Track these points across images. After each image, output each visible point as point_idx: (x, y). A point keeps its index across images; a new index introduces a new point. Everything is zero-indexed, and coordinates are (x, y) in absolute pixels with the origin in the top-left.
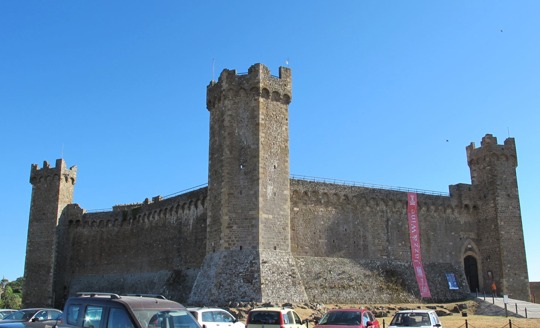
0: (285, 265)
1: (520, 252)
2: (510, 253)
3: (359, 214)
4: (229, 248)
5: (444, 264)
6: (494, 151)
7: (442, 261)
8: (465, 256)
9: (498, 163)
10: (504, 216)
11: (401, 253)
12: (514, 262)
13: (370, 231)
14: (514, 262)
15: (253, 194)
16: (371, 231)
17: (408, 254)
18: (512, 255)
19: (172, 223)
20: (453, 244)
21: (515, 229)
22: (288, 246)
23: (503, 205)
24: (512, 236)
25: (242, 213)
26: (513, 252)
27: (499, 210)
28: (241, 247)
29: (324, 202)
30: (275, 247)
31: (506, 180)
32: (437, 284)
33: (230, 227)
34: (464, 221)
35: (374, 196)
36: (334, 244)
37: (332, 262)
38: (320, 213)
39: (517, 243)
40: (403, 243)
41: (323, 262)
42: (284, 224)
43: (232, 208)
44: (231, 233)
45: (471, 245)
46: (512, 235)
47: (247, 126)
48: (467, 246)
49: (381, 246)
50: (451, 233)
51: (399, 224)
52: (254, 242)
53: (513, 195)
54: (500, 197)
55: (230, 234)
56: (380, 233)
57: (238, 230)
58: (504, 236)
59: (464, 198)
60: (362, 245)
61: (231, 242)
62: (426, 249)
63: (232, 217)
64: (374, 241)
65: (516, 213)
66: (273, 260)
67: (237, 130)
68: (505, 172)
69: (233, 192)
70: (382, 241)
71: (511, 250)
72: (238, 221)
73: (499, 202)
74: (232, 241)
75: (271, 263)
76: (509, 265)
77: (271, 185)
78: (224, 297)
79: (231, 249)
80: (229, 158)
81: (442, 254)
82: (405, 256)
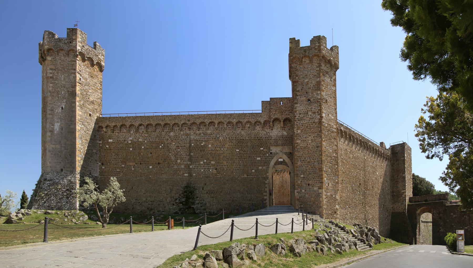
1: (316, 161)
2: (305, 162)
6: (294, 56)
9: (301, 68)
10: (302, 124)
11: (202, 170)
12: (309, 172)
14: (309, 172)
17: (210, 170)
18: (306, 164)
21: (313, 136)
23: (301, 112)
24: (308, 144)
26: (308, 161)
27: (297, 117)
31: (307, 83)
39: (314, 152)
46: (309, 144)
53: (313, 100)
54: (299, 104)
58: (299, 145)
64: (177, 161)
65: (315, 119)
68: (307, 75)
70: (184, 161)
71: (306, 159)
73: (297, 109)
76: (302, 176)
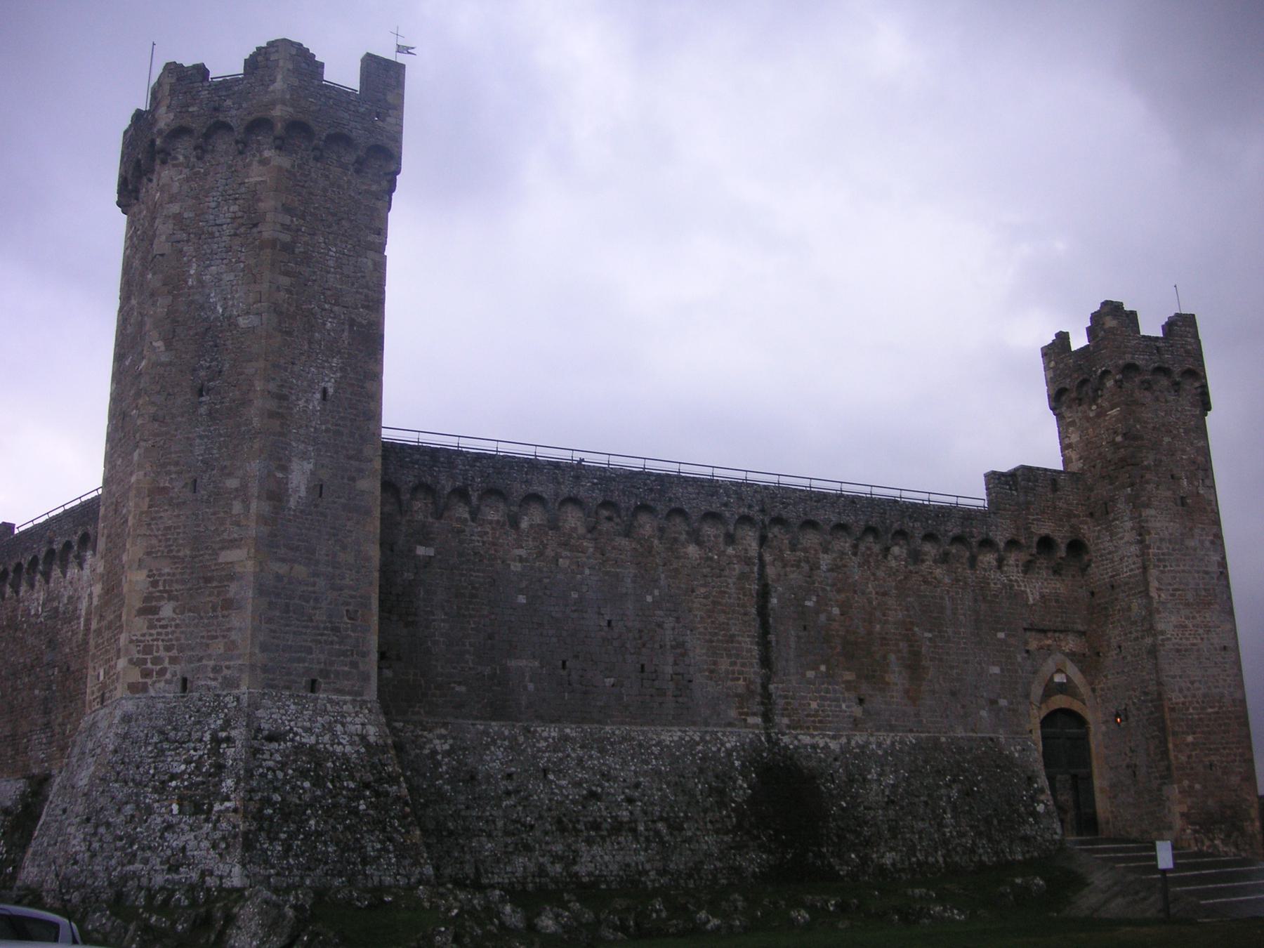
0: (348, 749)
3: (661, 569)
4: (144, 688)
5: (970, 739)
7: (966, 731)
8: (1044, 713)
13: (702, 630)
15: (237, 490)
16: (706, 629)
17: (840, 706)
19: (33, 612)
20: (1002, 670)
22: (365, 678)
25: (193, 557)
28: (185, 680)
29: (531, 526)
30: (314, 682)
32: (945, 812)
33: (148, 610)
34: (1040, 593)
35: (715, 507)
36: (564, 673)
37: (554, 738)
38: (516, 567)
40: (823, 668)
41: (521, 739)
42: (352, 597)
43: (160, 541)
44: (154, 632)
45: (1063, 675)
47: (227, 252)
48: (1052, 678)
49: (741, 682)
50: (996, 635)
51: (808, 603)
52: (232, 663)
55: (151, 635)
56: (738, 635)
57: (178, 622)
59: (1037, 514)
60: (669, 677)
61: (152, 663)
62: (907, 692)
63: (160, 575)
64: (715, 663)
66: (300, 730)
67: (194, 266)
69: (167, 485)
70: (743, 665)
72: (179, 587)
74: (156, 661)
75: (292, 740)
77: (304, 456)
78: (107, 869)
79: (152, 693)
80: (162, 364)
81: (963, 707)
82: (828, 716)
